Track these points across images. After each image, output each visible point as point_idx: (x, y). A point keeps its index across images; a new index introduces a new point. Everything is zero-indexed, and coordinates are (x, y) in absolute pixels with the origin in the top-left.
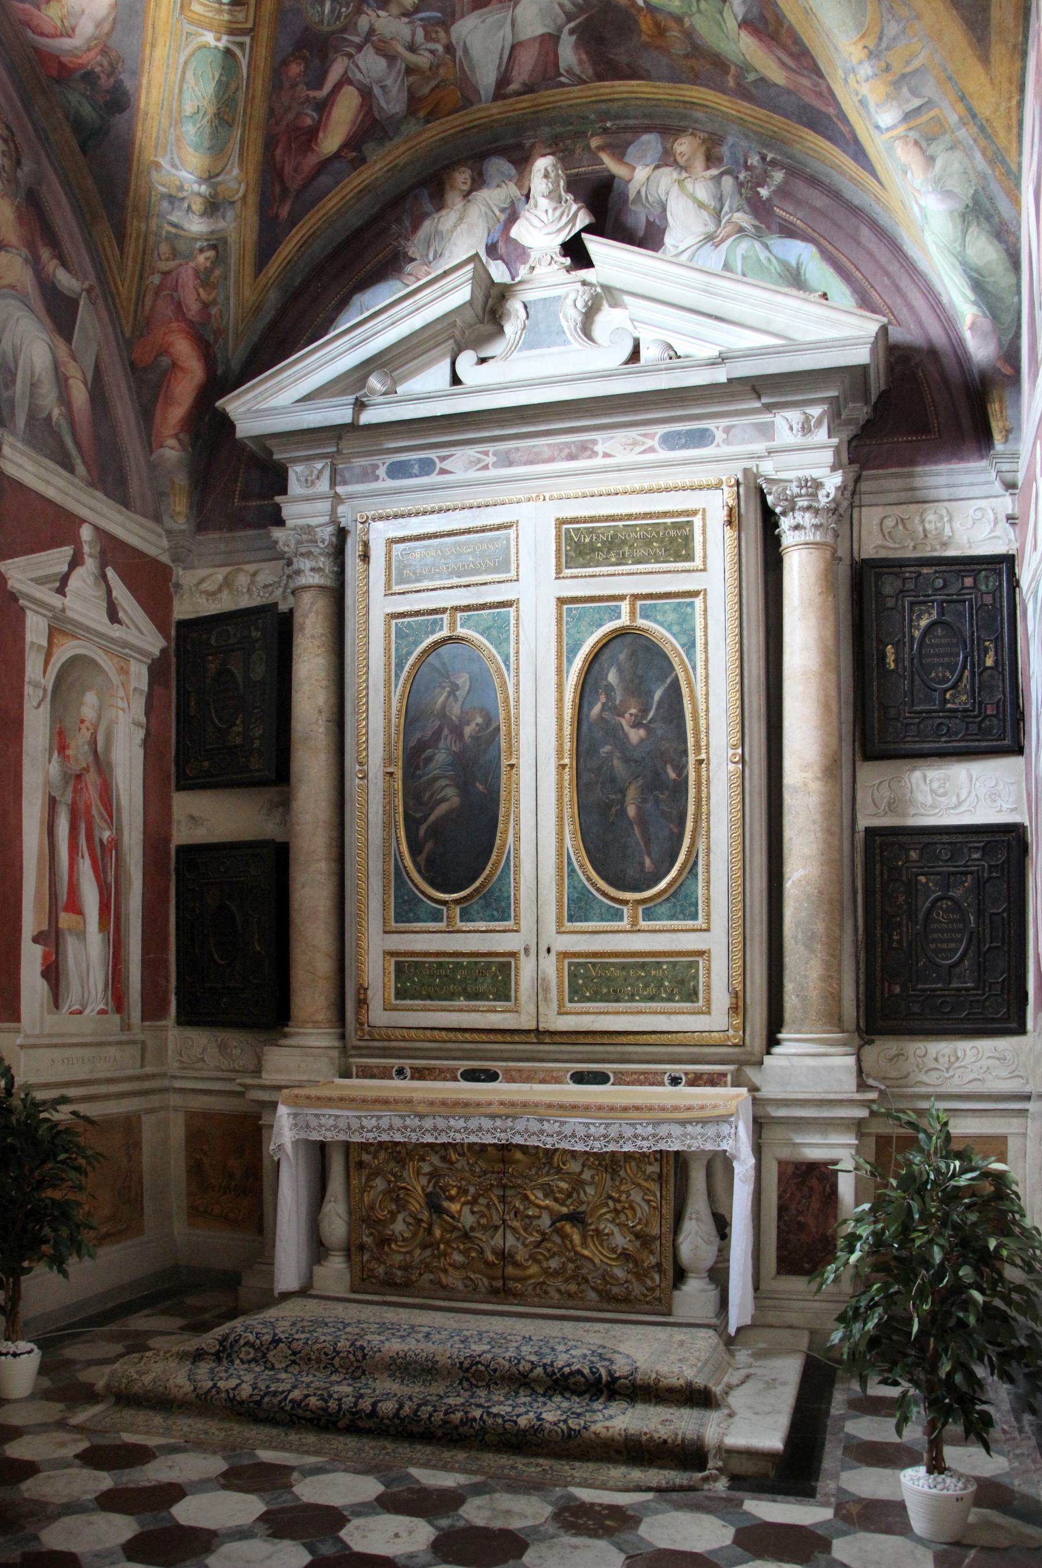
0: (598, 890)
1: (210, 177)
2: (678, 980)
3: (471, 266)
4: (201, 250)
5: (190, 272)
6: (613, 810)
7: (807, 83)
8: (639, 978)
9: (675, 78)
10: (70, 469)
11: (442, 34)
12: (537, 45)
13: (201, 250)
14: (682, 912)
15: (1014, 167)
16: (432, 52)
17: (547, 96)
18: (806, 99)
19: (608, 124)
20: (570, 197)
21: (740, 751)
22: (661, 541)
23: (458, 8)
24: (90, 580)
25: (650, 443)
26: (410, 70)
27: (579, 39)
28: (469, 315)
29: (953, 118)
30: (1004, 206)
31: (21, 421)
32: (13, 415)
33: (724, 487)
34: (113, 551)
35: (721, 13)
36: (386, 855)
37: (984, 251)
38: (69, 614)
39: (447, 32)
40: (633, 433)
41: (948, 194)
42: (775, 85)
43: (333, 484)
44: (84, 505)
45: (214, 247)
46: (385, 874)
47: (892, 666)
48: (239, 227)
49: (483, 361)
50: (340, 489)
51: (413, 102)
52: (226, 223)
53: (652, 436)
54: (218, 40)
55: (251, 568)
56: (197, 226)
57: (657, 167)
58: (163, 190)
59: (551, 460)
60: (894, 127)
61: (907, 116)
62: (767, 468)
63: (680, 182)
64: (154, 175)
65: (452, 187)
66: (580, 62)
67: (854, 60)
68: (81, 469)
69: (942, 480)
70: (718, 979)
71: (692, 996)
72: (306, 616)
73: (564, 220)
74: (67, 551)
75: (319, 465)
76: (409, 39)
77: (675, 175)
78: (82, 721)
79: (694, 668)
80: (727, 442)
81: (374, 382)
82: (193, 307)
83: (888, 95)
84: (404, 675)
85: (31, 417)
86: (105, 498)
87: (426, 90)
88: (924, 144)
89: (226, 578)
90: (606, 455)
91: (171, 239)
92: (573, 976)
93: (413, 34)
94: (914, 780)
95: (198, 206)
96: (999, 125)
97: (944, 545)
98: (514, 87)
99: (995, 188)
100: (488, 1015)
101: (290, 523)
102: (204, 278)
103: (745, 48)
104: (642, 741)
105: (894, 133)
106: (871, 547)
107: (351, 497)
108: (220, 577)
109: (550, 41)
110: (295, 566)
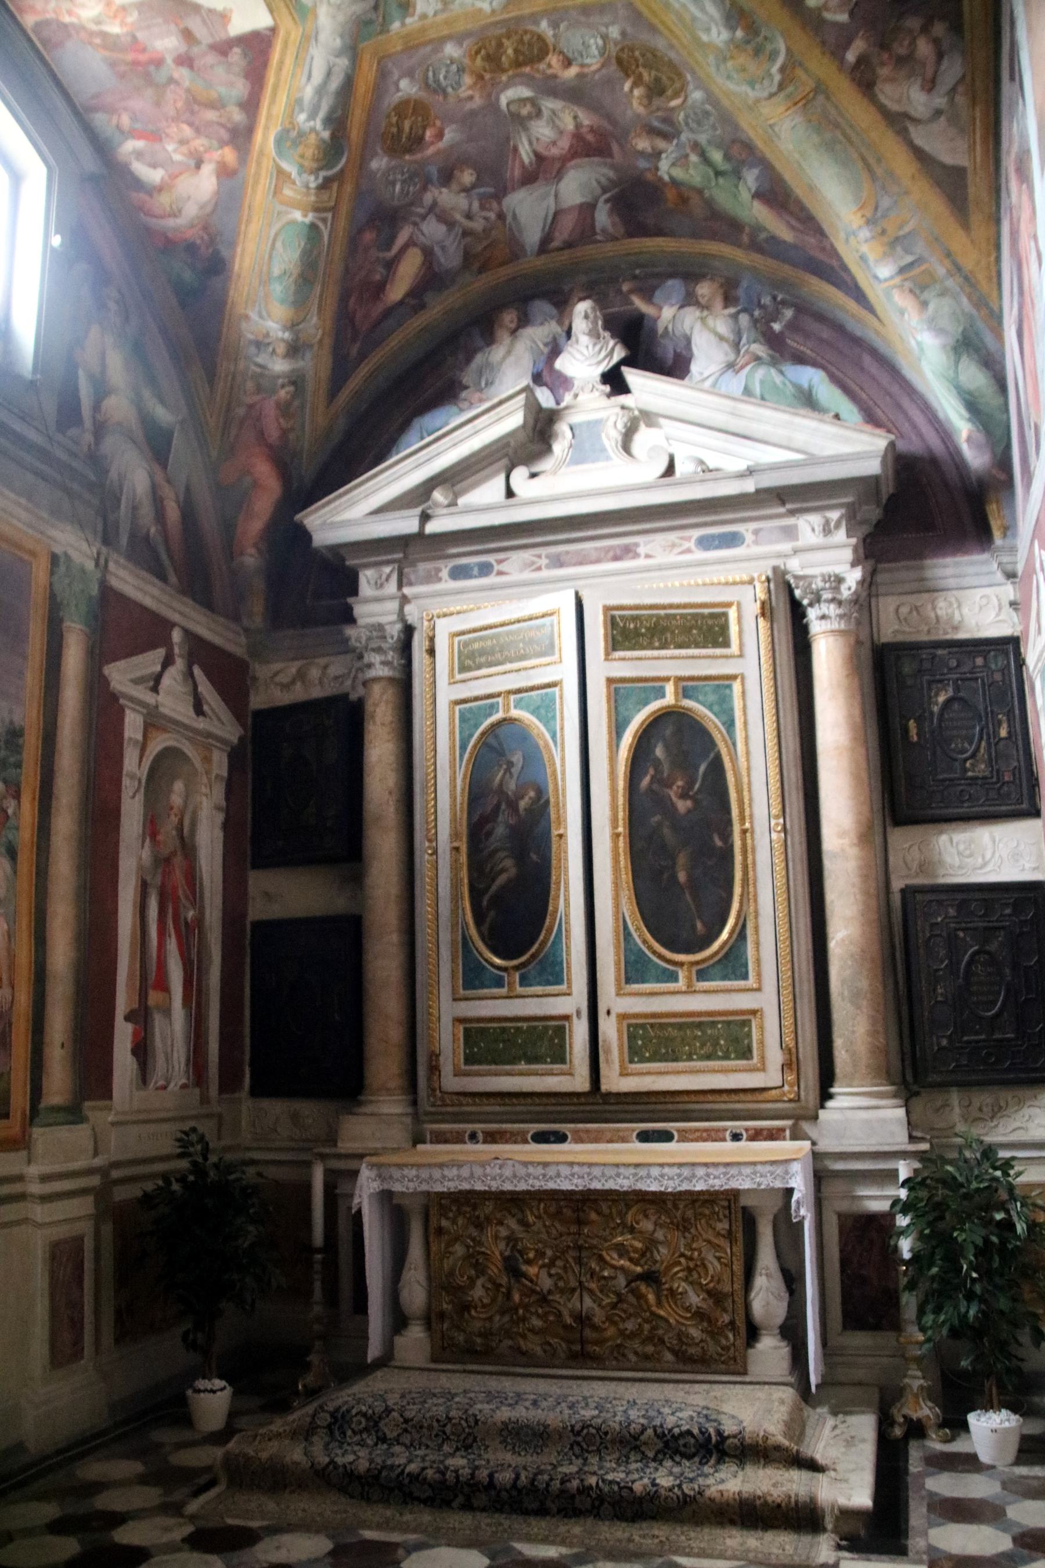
0: (654, 952)
1: (293, 325)
2: (732, 1038)
3: (523, 396)
4: (283, 386)
5: (272, 403)
6: (665, 876)
7: (813, 240)
8: (696, 1037)
9: (695, 235)
10: (163, 577)
11: (495, 205)
13: (283, 386)
14: (734, 973)
15: (996, 308)
16: (486, 219)
17: (588, 251)
18: (812, 253)
19: (637, 272)
20: (607, 334)
21: (781, 821)
22: (700, 629)
24: (179, 678)
25: (687, 545)
26: (465, 233)
28: (522, 437)
29: (941, 271)
30: (989, 339)
31: (124, 540)
32: (117, 534)
33: (756, 583)
34: (201, 652)
35: (737, 186)
36: (454, 926)
37: (974, 376)
38: (161, 709)
39: (500, 203)
40: (672, 536)
41: (940, 331)
42: (785, 242)
43: (400, 586)
44: (175, 610)
45: (293, 383)
46: (454, 943)
47: (915, 739)
48: (315, 365)
49: (533, 475)
50: (406, 590)
51: (468, 257)
52: (306, 363)
53: (689, 539)
54: (305, 216)
55: (322, 661)
56: (280, 366)
57: (681, 307)
58: (251, 337)
59: (598, 561)
60: (892, 278)
61: (902, 270)
62: (794, 566)
63: (703, 320)
64: (244, 325)
65: (501, 326)
66: (614, 224)
67: (855, 226)
68: (173, 579)
69: (949, 571)
70: (769, 1038)
71: (746, 1053)
72: (376, 705)
73: (603, 354)
74: (161, 652)
75: (387, 570)
77: (698, 313)
78: (172, 808)
79: (734, 744)
80: (756, 542)
81: (438, 496)
82: (273, 434)
83: (885, 254)
84: (466, 756)
85: (133, 536)
86: (190, 602)
87: (480, 248)
88: (918, 292)
89: (299, 671)
90: (648, 556)
91: (256, 377)
92: (632, 1037)
93: (470, 205)
94: (941, 843)
95: (281, 349)
96: (981, 277)
97: (956, 628)
98: (555, 244)
99: (980, 325)
100: (545, 1078)
101: (361, 622)
102: (284, 409)
103: (760, 213)
104: (689, 811)
105: (892, 282)
106: (889, 631)
107: (417, 597)
108: (294, 670)
109: (588, 209)
110: (366, 660)
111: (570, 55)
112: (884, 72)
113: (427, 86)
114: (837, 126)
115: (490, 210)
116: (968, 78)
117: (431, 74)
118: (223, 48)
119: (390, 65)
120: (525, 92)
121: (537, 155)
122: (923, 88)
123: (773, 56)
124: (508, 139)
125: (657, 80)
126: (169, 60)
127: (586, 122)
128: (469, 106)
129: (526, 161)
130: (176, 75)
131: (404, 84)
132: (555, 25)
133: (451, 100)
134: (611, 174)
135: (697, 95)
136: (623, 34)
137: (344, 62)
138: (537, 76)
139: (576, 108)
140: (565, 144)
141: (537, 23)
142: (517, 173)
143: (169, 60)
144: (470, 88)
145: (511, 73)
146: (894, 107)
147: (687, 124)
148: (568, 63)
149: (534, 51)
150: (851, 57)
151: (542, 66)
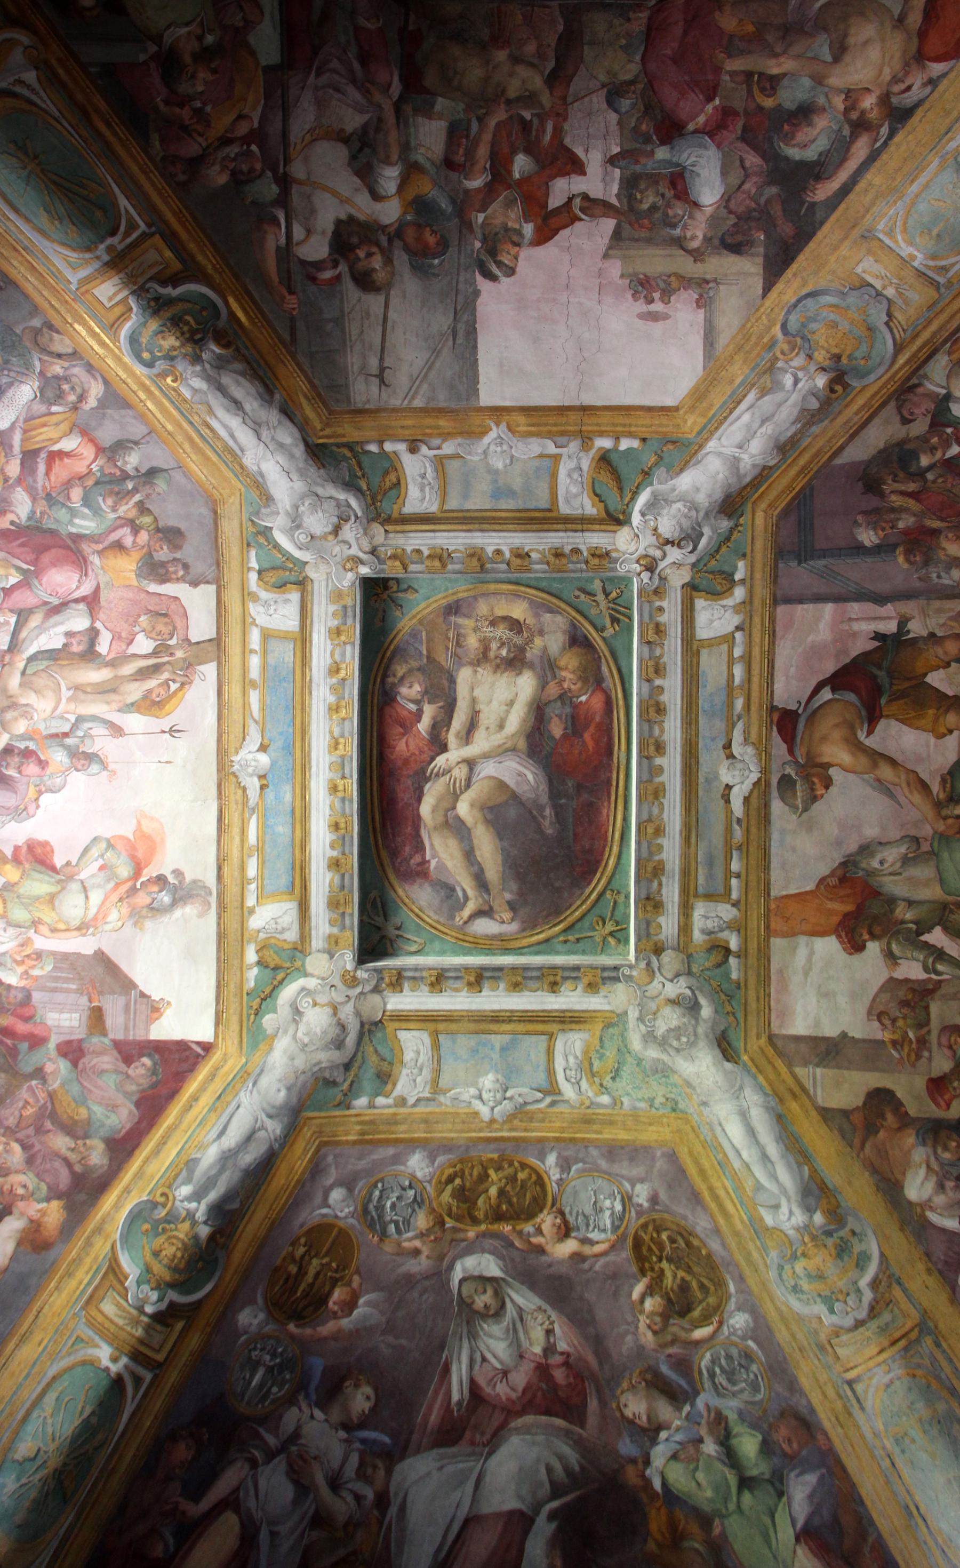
11: (381, 1473)
12: (500, 1528)
16: (358, 1498)
23: (415, 1438)
27: (559, 1530)
39: (389, 1472)
76: (336, 1465)
93: (345, 1459)
109: (519, 1523)
111: (571, 1219)
113: (365, 1211)
115: (369, 1481)
117: (377, 1193)
118: (128, 1052)
119: (330, 1158)
120: (491, 1266)
121: (474, 1386)
124: (442, 1347)
126: (52, 1045)
127: (562, 1346)
129: (455, 1397)
130: (49, 1068)
131: (336, 1195)
132: (565, 1165)
133: (388, 1247)
134: (573, 1457)
136: (654, 1199)
137: (275, 1128)
138: (517, 1243)
139: (554, 1317)
140: (520, 1378)
141: (542, 1157)
142: (434, 1418)
143: (52, 1045)
144: (421, 1235)
145: (483, 1227)
148: (565, 1231)
149: (527, 1198)
151: (529, 1228)
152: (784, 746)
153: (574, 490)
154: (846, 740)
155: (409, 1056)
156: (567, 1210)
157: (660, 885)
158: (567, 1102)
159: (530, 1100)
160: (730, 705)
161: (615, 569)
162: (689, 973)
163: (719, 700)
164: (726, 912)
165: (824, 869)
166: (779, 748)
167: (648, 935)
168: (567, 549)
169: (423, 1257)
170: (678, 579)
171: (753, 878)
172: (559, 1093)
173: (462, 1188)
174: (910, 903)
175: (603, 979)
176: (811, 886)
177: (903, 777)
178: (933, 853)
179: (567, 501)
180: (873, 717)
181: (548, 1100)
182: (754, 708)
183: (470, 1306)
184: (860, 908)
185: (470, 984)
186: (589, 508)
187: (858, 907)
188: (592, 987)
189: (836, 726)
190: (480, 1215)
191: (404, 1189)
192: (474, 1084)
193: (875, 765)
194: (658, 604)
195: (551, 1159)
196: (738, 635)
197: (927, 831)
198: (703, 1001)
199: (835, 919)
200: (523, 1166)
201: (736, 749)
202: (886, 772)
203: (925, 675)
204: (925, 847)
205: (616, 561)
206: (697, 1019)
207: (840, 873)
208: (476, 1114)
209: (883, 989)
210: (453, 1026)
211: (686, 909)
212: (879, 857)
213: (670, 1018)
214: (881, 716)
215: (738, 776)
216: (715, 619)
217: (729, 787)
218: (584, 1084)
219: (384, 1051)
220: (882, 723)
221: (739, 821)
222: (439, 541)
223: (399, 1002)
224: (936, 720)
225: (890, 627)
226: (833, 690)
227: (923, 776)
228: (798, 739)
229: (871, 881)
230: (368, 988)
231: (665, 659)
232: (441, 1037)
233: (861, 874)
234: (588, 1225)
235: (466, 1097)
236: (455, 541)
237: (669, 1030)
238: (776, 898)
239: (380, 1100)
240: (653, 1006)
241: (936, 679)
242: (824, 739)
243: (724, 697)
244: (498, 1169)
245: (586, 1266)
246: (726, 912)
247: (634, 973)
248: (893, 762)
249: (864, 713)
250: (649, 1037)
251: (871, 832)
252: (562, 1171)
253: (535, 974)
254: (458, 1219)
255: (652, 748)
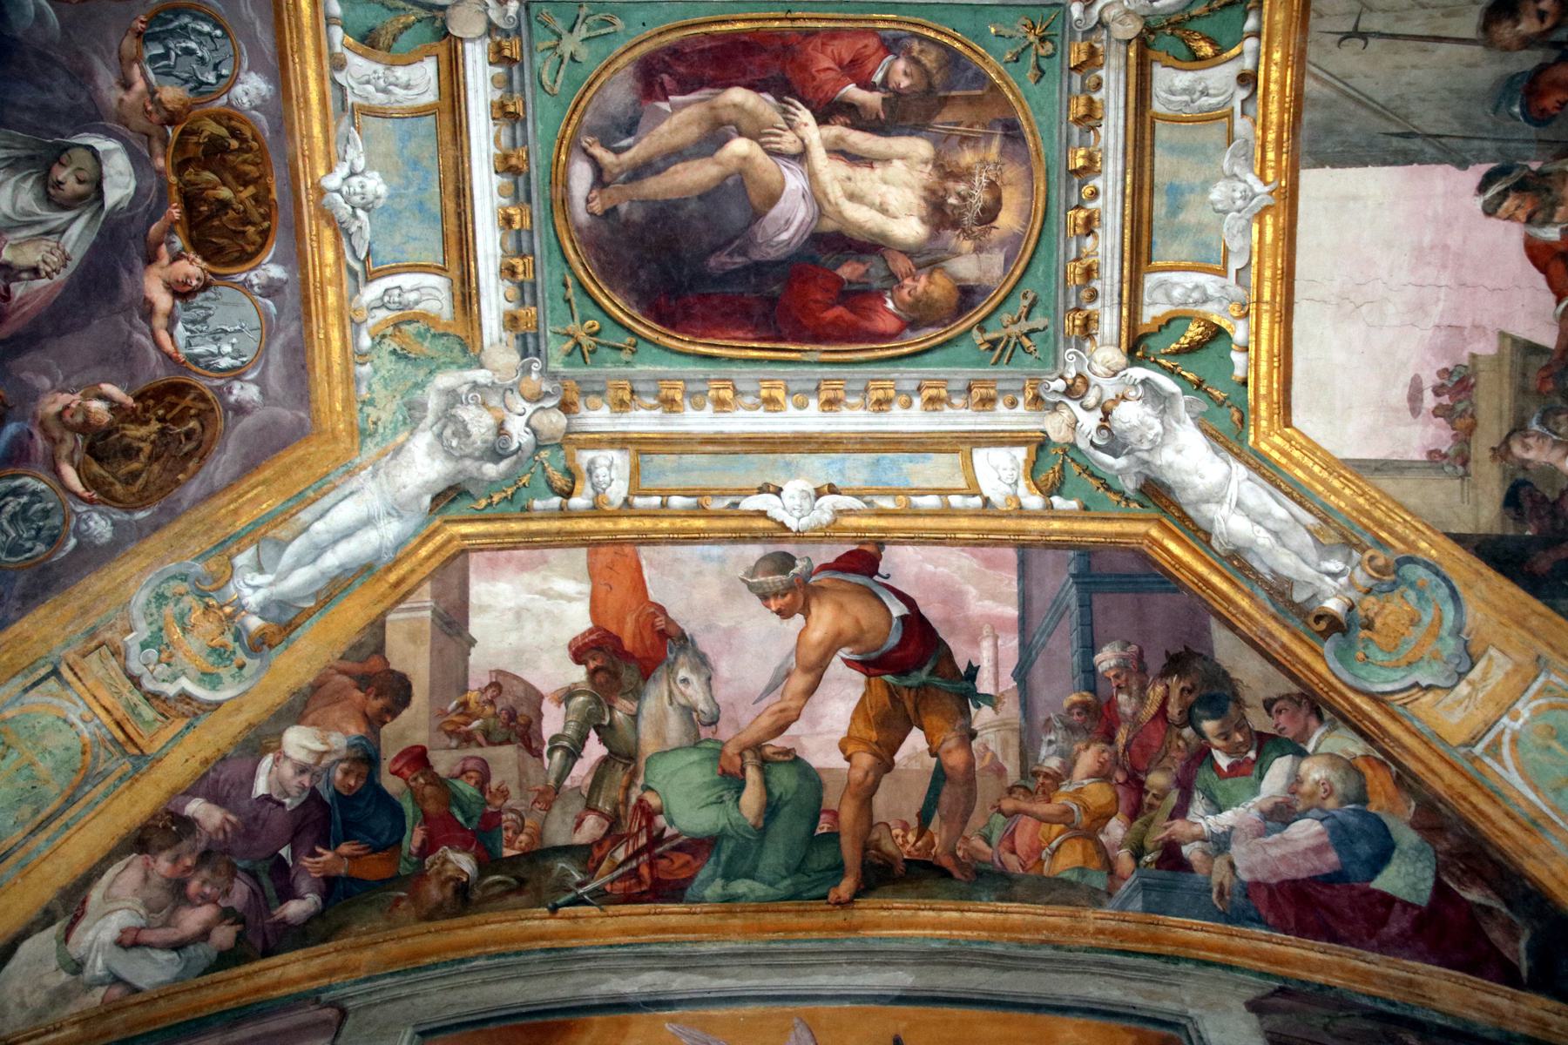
112: (163, 864)
114: (70, 801)
116: (139, 998)
117: (206, 28)
122: (124, 931)
123: (209, 678)
125: (130, 452)
127: (18, 290)
128: (106, 79)
132: (272, 289)
133: (130, 45)
135: (100, 526)
144: (152, 92)
145: (173, 179)
146: (95, 895)
147: (16, 492)
148: (181, 292)
149: (223, 238)
150: (196, 807)
151: (179, 243)
152: (831, 560)
153: (1177, 293)
154: (839, 634)
155: (401, 73)
156: (209, 294)
157: (652, 408)
158: (358, 291)
159: (355, 241)
160: (884, 493)
161: (1067, 345)
162: (539, 447)
163: (893, 479)
164: (617, 492)
165: (677, 609)
166: (829, 553)
167: (585, 394)
168: (1096, 284)
169: (121, 93)
170: (1054, 427)
171: (665, 524)
172: (368, 281)
173: (226, 150)
174: (635, 717)
175: (524, 336)
176: (653, 596)
177: (793, 704)
178: (696, 743)
179: (1161, 284)
180: (869, 666)
181: (357, 267)
182: (882, 522)
183: (58, 159)
184: (627, 656)
185: (506, 157)
186: (1151, 313)
187: (629, 652)
188: (511, 321)
189: (857, 622)
190: (190, 175)
191: (216, 67)
192: (370, 166)
193: (807, 670)
194: (1021, 400)
195: (276, 272)
196: (977, 501)
197: (725, 732)
198: (504, 465)
199: (613, 629)
200: (265, 234)
201: (828, 501)
202: (799, 682)
203: (921, 727)
204: (705, 733)
205: (1080, 346)
206: (480, 458)
207: (671, 629)
208: (330, 170)
209: (529, 687)
210: (447, 137)
211: (620, 442)
212: (693, 678)
213: (480, 424)
214: (869, 675)
215: (795, 502)
216: (1000, 473)
217: (778, 492)
218: (382, 314)
219: (405, 40)
220: (860, 678)
221: (736, 505)
222: (1112, 114)
223: (476, 58)
224: (862, 741)
225: (985, 685)
226: (903, 618)
227: (793, 729)
228: (840, 576)
229: (663, 667)
230: (494, 15)
231: (947, 410)
232: (430, 119)
233: (671, 656)
234: (194, 322)
235: (351, 153)
236: (1113, 131)
237: (464, 424)
238: (636, 554)
239: (338, 33)
240: (495, 401)
241: (916, 740)
242: (841, 607)
243: (896, 484)
244: (255, 198)
245: (137, 320)
246: (617, 492)
247: (534, 376)
248: (810, 691)
249: (874, 655)
250: (453, 397)
251: (723, 668)
252: (262, 287)
253: (525, 245)
254: (181, 143)
255: (831, 394)
